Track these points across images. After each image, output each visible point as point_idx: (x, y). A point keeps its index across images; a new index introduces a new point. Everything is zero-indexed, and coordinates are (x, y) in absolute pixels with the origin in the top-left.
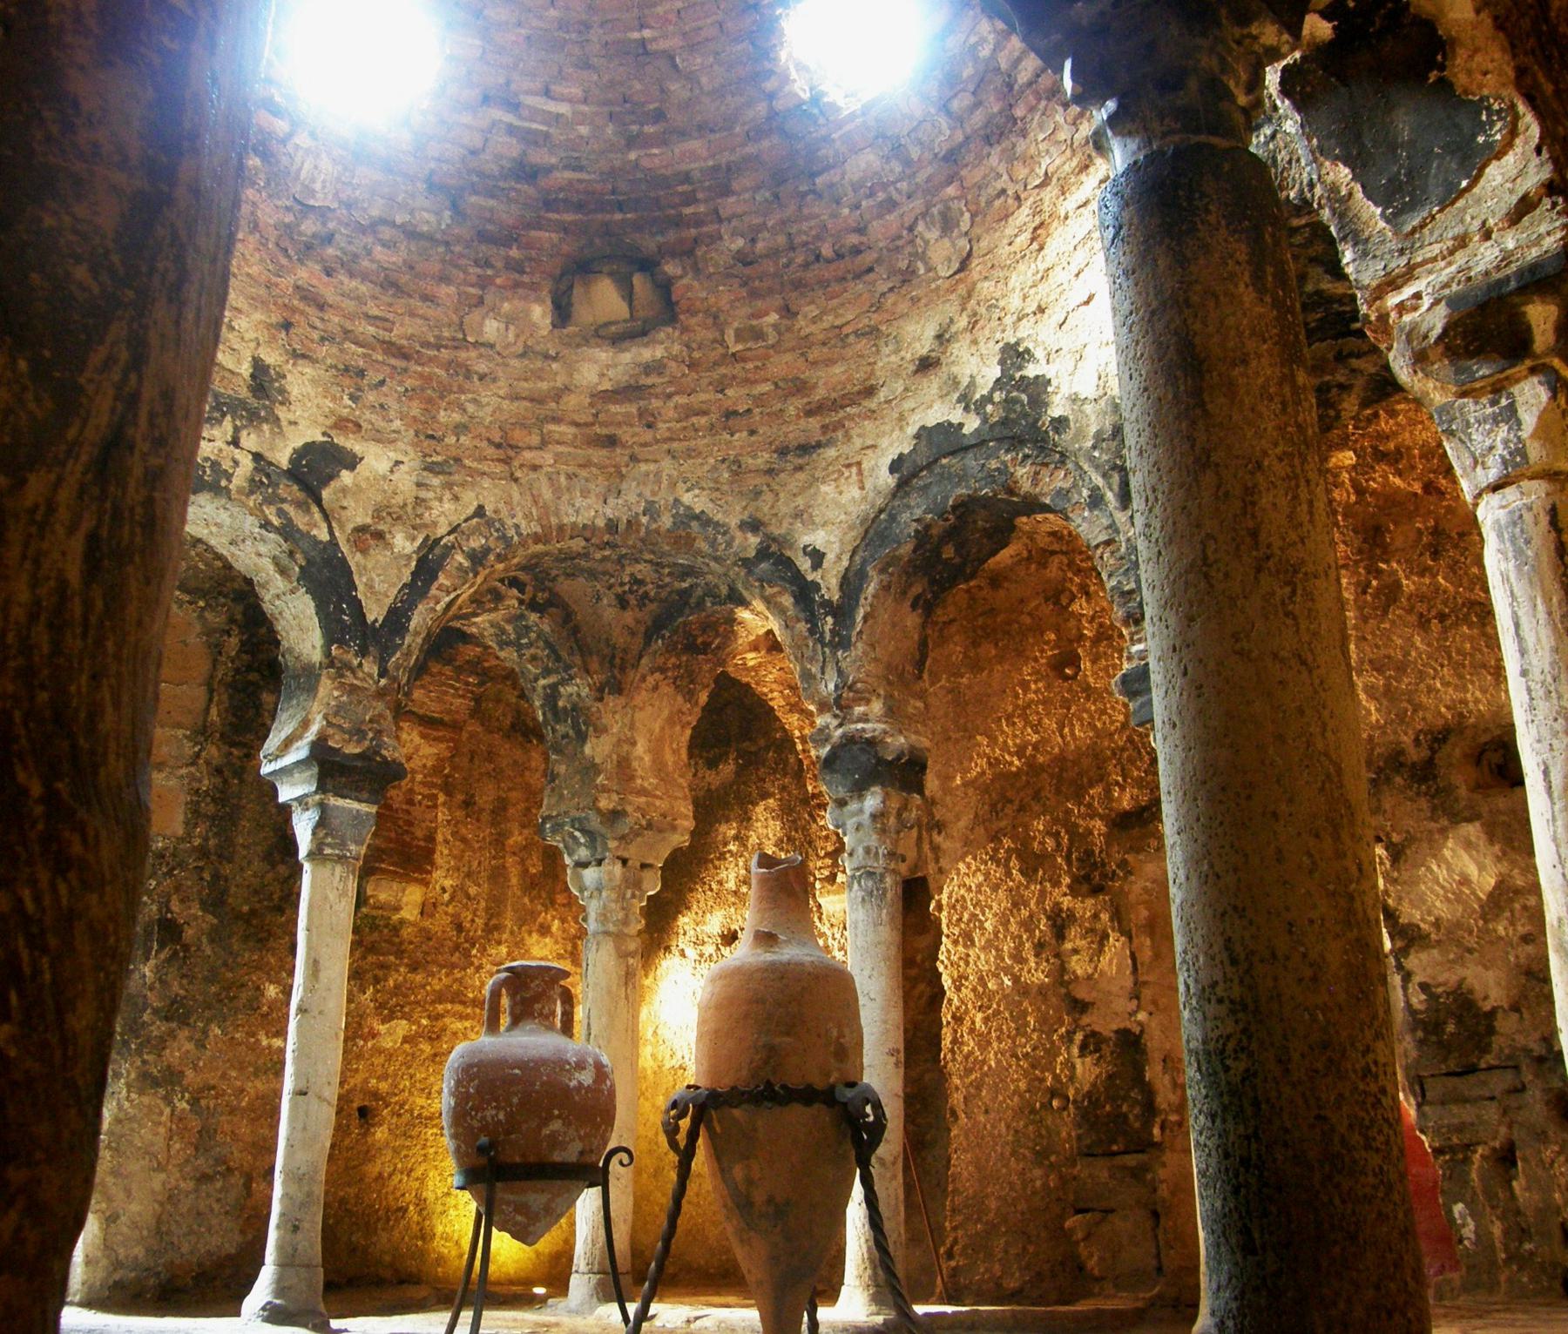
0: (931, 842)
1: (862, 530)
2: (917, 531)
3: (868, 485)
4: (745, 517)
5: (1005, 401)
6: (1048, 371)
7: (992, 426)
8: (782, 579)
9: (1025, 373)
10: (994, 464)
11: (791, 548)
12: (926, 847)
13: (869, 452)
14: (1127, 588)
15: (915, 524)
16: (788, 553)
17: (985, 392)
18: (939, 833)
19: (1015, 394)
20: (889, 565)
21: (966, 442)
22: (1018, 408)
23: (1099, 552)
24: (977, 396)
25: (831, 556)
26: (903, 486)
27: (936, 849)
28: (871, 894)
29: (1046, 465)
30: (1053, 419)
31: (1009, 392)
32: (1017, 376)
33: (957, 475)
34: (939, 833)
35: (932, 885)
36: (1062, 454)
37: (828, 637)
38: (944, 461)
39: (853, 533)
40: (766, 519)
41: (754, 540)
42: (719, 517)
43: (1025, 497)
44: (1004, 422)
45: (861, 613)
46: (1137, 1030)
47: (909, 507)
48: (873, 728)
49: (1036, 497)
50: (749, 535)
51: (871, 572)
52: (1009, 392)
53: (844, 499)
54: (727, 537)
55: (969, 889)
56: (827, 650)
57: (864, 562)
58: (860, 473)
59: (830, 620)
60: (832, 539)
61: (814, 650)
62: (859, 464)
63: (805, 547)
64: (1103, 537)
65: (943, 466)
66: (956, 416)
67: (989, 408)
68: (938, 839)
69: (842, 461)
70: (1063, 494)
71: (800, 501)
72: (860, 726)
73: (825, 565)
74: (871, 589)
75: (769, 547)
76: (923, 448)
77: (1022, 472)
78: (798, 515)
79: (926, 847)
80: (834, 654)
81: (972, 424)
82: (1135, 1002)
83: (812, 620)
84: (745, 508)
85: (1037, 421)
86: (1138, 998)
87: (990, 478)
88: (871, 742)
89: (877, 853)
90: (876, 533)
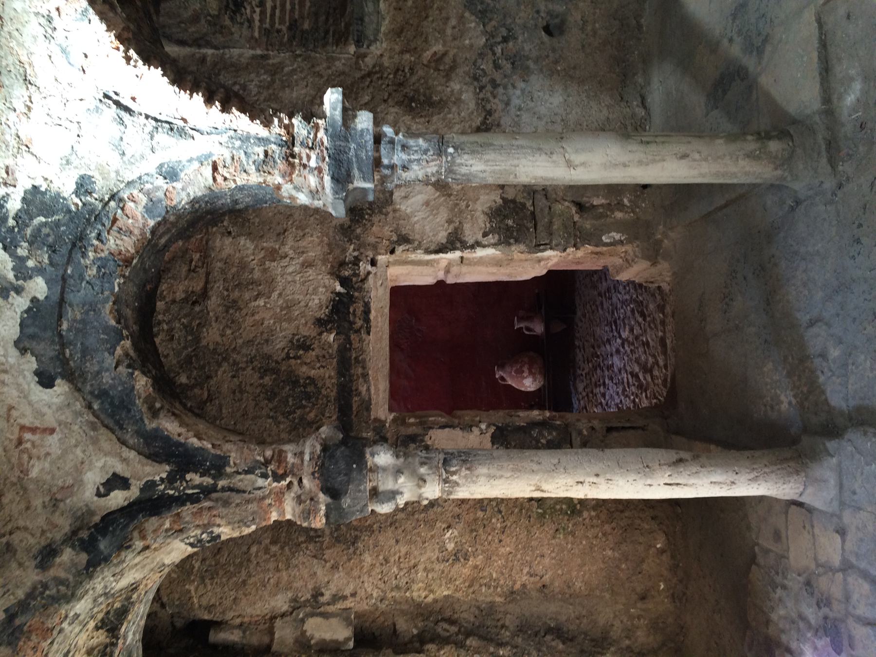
0: (328, 604)
1: (103, 430)
2: (129, 366)
3: (50, 420)
4: (31, 564)
5: (31, 244)
6: (24, 184)
7: (51, 264)
8: (126, 526)
9: (12, 214)
10: (94, 271)
11: (91, 513)
12: (331, 609)
13: (14, 413)
14: (262, 156)
15: (120, 368)
16: (97, 519)
17: (10, 265)
18: (322, 595)
19: (29, 231)
20: (151, 408)
21: (56, 298)
22: (46, 230)
23: (219, 179)
24: (11, 276)
25: (120, 469)
26: (70, 376)
27: (337, 598)
28: (464, 461)
29: (115, 220)
30: (77, 193)
31: (24, 237)
32: (11, 222)
33: (87, 313)
34: (322, 595)
35: (364, 607)
36: (113, 197)
37: (208, 481)
38: (65, 326)
39: (103, 438)
40: (43, 543)
41: (67, 555)
42: (21, 594)
43: (137, 252)
44: (52, 249)
45: (195, 442)
46: (492, 429)
47: (98, 373)
48: (311, 447)
49: (143, 234)
50: (58, 560)
51: (150, 425)
52: (24, 237)
53: (56, 451)
54: (51, 584)
55: (373, 566)
56: (221, 483)
57: (141, 433)
58: (33, 430)
59: (188, 477)
60: (99, 464)
61: (217, 500)
62: (23, 428)
63: (99, 495)
64: (208, 171)
65: (69, 330)
66: (21, 303)
67: (31, 263)
68: (326, 598)
69: (11, 446)
70: (148, 210)
71: (37, 502)
72: (307, 457)
73: (127, 475)
74: (170, 427)
75: (82, 541)
76: (40, 347)
77: (112, 242)
78: (55, 503)
79: (331, 609)
80: (229, 476)
81: (39, 287)
82: (474, 429)
83: (182, 500)
84: (20, 565)
85: (69, 211)
86: (471, 426)
87: (104, 276)
88: (325, 448)
89: (425, 458)
90: (112, 416)
